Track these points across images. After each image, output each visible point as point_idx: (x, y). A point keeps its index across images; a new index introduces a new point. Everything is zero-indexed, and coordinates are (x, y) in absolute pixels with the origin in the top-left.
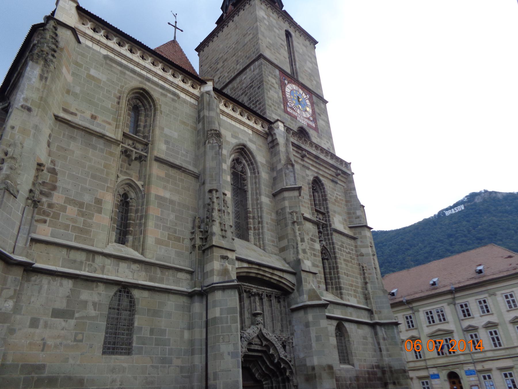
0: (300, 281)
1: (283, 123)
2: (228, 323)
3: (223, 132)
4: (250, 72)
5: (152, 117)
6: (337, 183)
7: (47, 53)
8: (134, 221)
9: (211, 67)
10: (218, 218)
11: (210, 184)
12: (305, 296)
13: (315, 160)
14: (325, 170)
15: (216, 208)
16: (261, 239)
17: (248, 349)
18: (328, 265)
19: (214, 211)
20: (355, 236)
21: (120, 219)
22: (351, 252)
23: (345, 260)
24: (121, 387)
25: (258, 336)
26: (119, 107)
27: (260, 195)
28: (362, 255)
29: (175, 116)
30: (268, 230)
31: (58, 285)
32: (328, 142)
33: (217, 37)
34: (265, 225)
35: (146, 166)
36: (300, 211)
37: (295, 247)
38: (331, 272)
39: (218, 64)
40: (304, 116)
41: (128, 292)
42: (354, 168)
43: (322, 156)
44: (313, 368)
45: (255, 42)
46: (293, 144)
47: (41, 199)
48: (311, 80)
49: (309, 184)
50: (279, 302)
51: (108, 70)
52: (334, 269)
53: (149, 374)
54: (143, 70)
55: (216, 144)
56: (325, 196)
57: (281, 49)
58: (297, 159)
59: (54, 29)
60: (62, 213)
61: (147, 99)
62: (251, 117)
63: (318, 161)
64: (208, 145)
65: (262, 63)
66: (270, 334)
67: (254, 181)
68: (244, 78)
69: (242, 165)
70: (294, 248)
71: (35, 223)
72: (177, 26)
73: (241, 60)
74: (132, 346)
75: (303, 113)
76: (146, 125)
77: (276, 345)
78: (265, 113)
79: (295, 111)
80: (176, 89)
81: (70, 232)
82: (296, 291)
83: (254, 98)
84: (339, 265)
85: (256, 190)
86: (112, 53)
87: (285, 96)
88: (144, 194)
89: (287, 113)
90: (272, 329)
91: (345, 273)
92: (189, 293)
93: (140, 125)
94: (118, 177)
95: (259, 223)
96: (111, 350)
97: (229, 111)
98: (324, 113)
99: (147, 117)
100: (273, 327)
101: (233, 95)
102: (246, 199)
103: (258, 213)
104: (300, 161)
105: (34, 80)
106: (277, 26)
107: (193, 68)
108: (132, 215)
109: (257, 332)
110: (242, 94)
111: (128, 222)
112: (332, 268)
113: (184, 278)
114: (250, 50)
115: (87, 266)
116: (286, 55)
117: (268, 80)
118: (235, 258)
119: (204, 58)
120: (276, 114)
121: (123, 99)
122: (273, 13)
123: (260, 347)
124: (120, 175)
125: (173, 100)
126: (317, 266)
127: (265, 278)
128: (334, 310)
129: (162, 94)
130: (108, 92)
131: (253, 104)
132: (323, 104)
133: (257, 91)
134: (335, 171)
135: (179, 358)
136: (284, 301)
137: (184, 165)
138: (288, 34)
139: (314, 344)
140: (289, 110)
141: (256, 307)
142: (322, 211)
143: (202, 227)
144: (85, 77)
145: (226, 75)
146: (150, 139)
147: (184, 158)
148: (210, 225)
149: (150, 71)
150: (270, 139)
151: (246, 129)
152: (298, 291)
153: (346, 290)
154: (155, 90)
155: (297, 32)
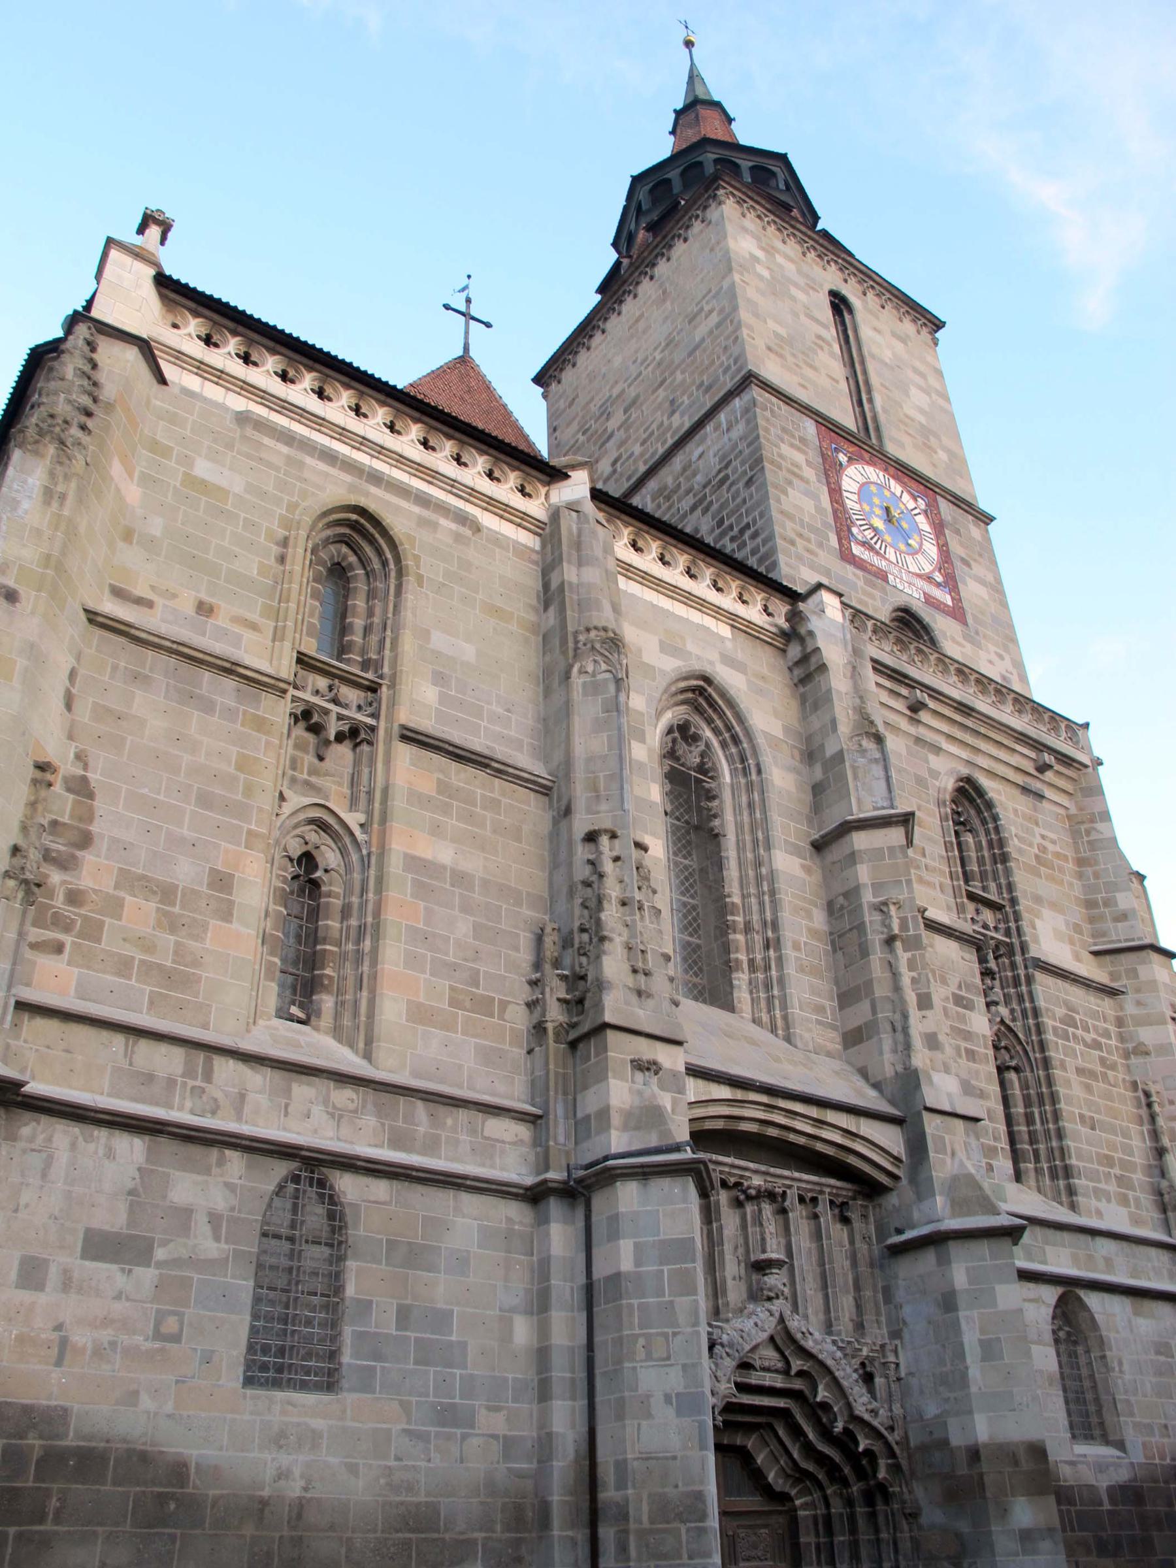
0: (918, 1146)
1: (840, 595)
2: (664, 1296)
3: (630, 634)
4: (714, 435)
5: (391, 598)
6: (1040, 797)
7: (66, 422)
8: (336, 946)
9: (588, 430)
10: (620, 927)
11: (589, 811)
12: (938, 1198)
13: (958, 718)
15: (614, 894)
16: (777, 1002)
17: (737, 1385)
18: (1022, 1089)
19: (606, 904)
20: (1114, 985)
21: (292, 940)
22: (1103, 1040)
23: (1080, 1071)
24: (308, 1495)
25: (772, 1339)
26: (284, 571)
27: (768, 848)
28: (1141, 1051)
29: (463, 590)
30: (801, 969)
31: (101, 1152)
32: (1001, 657)
33: (603, 332)
34: (788, 951)
35: (372, 762)
36: (912, 899)
37: (899, 1027)
38: (1032, 1113)
39: (608, 419)
40: (913, 568)
41: (322, 1183)
42: (1099, 742)
43: (983, 705)
44: (974, 1454)
45: (727, 338)
46: (879, 667)
47: (47, 876)
48: (930, 447)
49: (940, 803)
50: (845, 1220)
51: (249, 456)
52: (1041, 1103)
53: (398, 1459)
54: (359, 449)
55: (608, 675)
56: (1001, 843)
57: (819, 351)
58: (892, 718)
59: (86, 349)
60: (108, 920)
61: (372, 541)
62: (726, 583)
63: (969, 723)
64: (580, 681)
65: (754, 403)
66: (817, 1335)
67: (744, 799)
68: (696, 454)
69: (703, 747)
70: (894, 1030)
71: (28, 954)
72: (473, 313)
73: (685, 398)
74: (340, 1364)
75: (909, 559)
76: (371, 624)
77: (837, 1374)
78: (774, 565)
79: (877, 553)
80: (468, 501)
81: (133, 982)
82: (904, 1182)
83: (733, 519)
84: (1061, 1090)
85: (753, 831)
86: (262, 404)
87: (843, 505)
88: (369, 855)
89: (850, 563)
90: (822, 1316)
91: (1082, 1116)
92: (527, 1189)
93: (351, 624)
94: (282, 797)
95: (767, 947)
96: (271, 1374)
97: (647, 562)
98: (981, 555)
99: (374, 598)
100: (827, 1310)
101: (664, 514)
102: (719, 864)
103: (762, 911)
104: (904, 724)
105: (26, 505)
106: (802, 281)
107: (526, 438)
108: (332, 924)
109: (770, 1325)
110: (693, 509)
111: (319, 947)
112: (1035, 1099)
113: (508, 1137)
114: (713, 362)
115: (188, 1093)
116: (839, 370)
117: (780, 456)
118: (683, 1070)
119: (562, 404)
120: (813, 567)
121: (295, 547)
122: (784, 242)
123: (780, 1377)
124: (287, 793)
125: (458, 537)
126: (982, 1095)
127: (792, 1137)
128: (1048, 1248)
129: (423, 522)
130: (250, 524)
131: (733, 539)
132: (978, 527)
133: (744, 494)
134: (1033, 755)
135: (497, 1409)
136: (865, 1216)
137: (501, 751)
138: (839, 304)
139: (975, 1372)
140: (857, 550)
141: (763, 1239)
142: (993, 896)
143: (567, 961)
144: (178, 485)
145: (637, 449)
146: (386, 670)
147: (498, 729)
148: (592, 955)
149: (381, 450)
150: (794, 651)
151: (709, 622)
152: (913, 1180)
153: (1087, 1178)
154: (398, 509)
155: (870, 295)
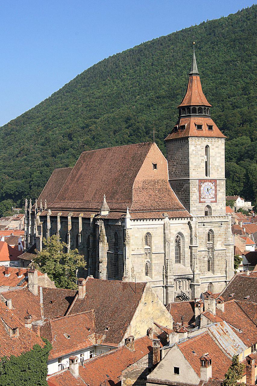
14: (215, 224)
28: (227, 256)
40: (210, 197)
98: (222, 187)
120: (194, 207)
129: (153, 230)
140: (201, 200)
151: (180, 225)
